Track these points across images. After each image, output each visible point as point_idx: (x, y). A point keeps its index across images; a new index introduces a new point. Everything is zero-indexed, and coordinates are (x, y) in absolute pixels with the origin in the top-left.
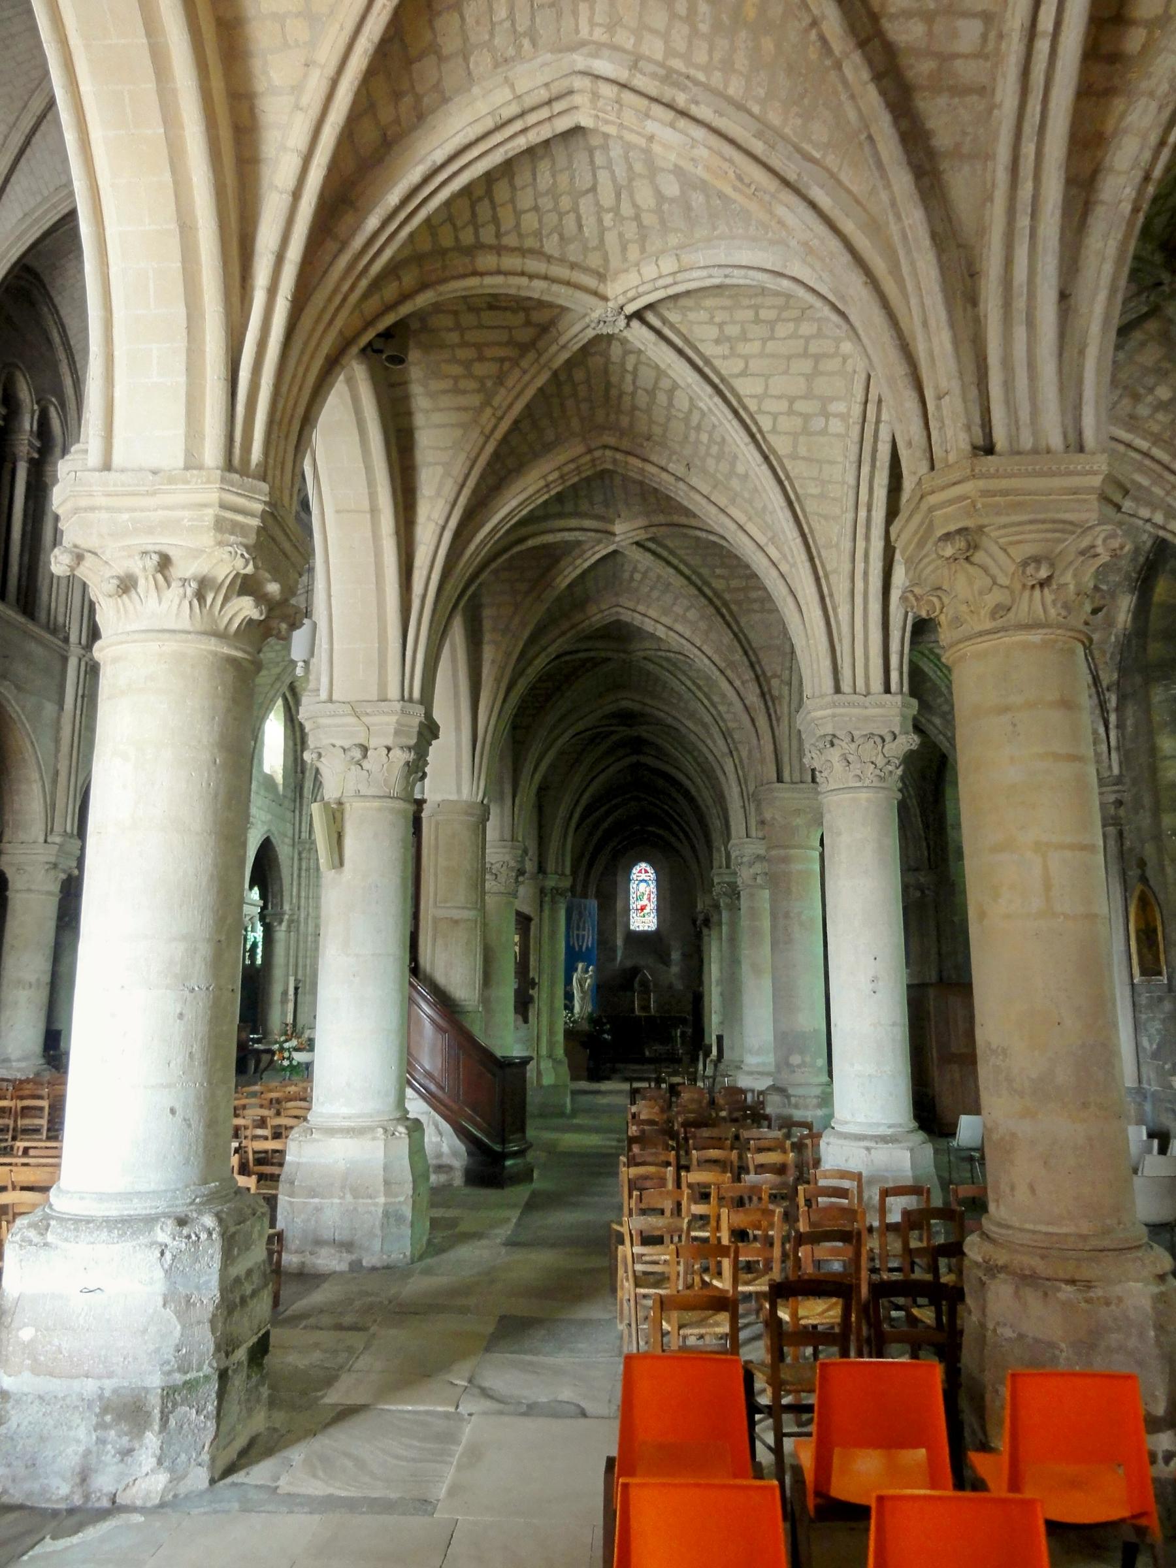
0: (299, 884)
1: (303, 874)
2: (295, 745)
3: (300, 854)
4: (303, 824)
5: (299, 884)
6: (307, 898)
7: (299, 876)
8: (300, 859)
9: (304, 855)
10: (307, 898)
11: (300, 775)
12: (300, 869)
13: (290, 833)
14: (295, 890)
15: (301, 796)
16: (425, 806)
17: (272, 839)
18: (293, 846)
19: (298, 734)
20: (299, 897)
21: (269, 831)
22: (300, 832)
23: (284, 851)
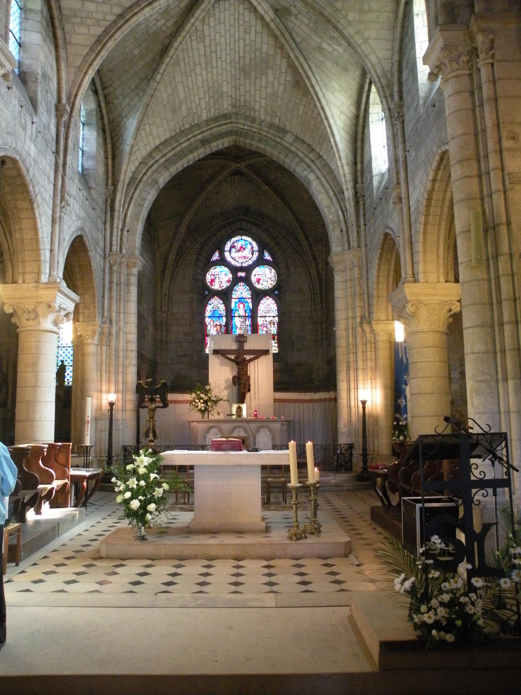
0: (110, 298)
1: (114, 287)
2: (106, 158)
3: (111, 267)
4: (114, 238)
5: (110, 298)
6: (118, 312)
7: (110, 290)
8: (111, 273)
9: (115, 268)
10: (118, 312)
11: (111, 188)
13: (101, 243)
14: (106, 303)
15: (112, 210)
17: (85, 238)
18: (104, 258)
19: (109, 146)
20: (110, 310)
21: (82, 229)
22: (111, 245)
23: (96, 259)
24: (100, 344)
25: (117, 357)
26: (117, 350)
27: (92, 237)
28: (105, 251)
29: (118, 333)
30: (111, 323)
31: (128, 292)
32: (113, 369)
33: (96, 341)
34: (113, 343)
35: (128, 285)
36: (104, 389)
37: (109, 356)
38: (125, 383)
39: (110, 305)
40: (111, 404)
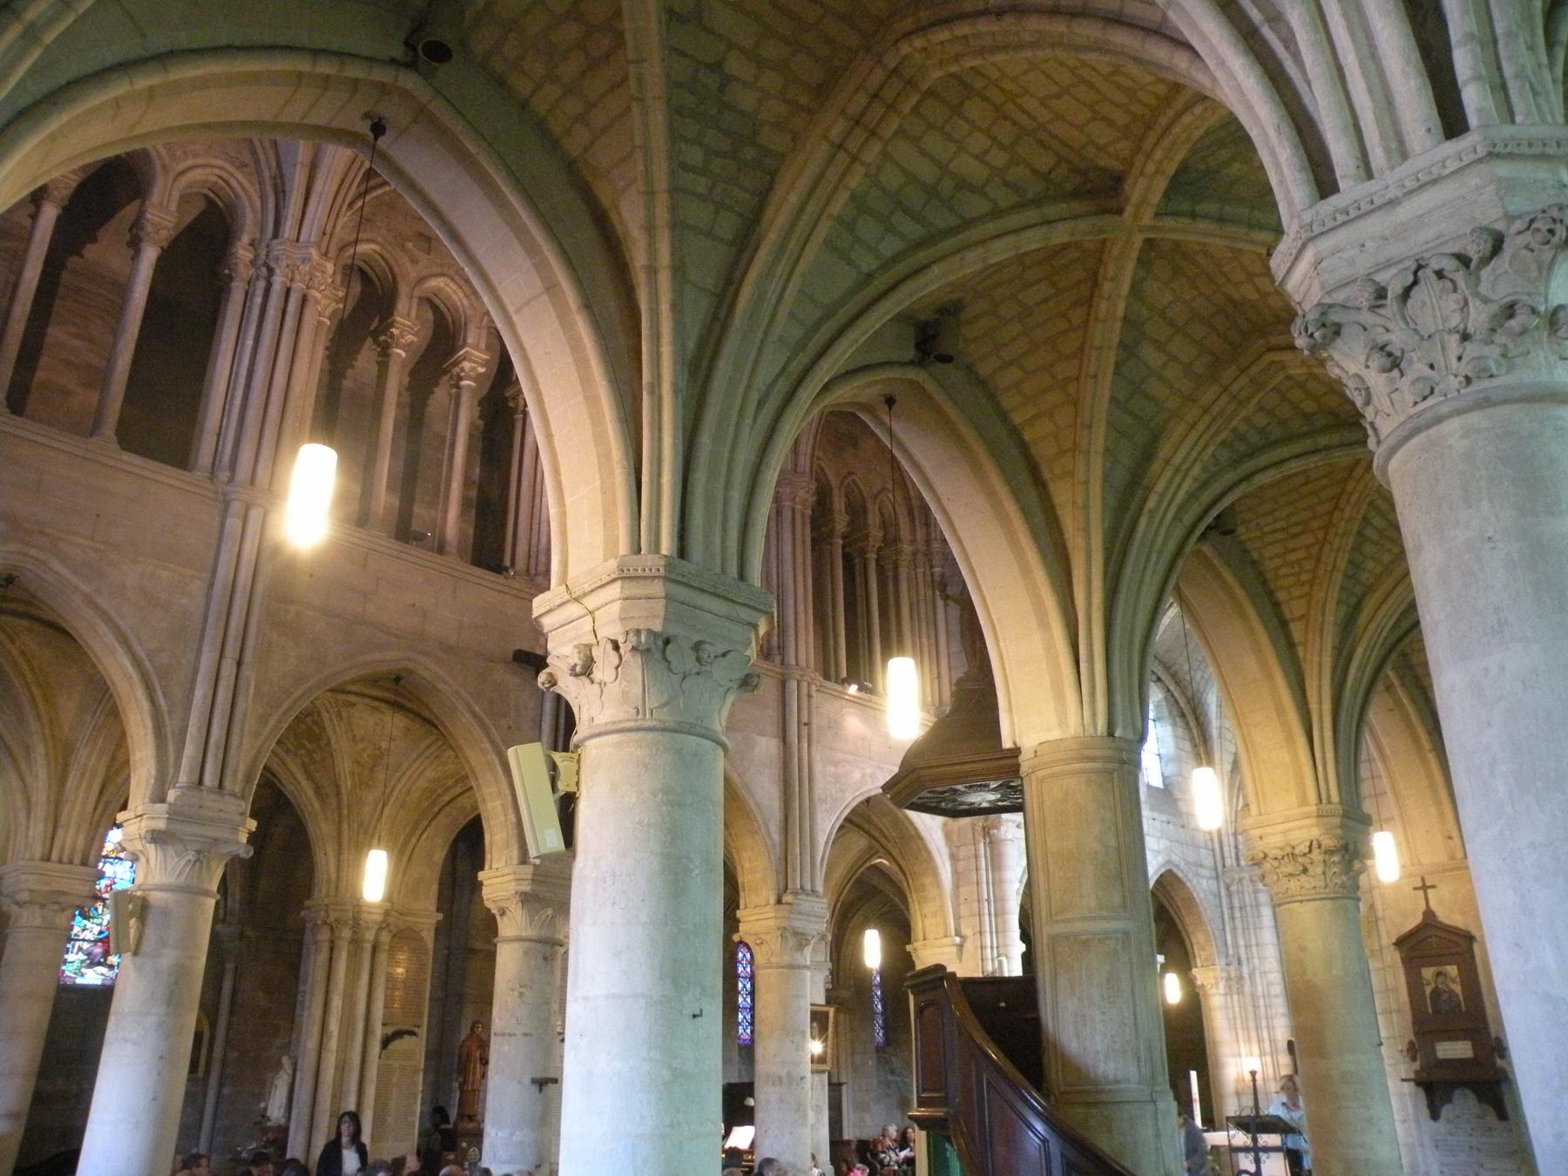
0: (1234, 929)
1: (1237, 914)
3: (1228, 888)
5: (1234, 929)
7: (1232, 918)
8: (1230, 895)
9: (1234, 888)
12: (1232, 908)
14: (1229, 937)
16: (1021, 758)
18: (1217, 878)
20: (1236, 945)
21: (1169, 862)
22: (1223, 858)
24: (1229, 992)
25: (1255, 1007)
26: (1254, 997)
27: (1187, 863)
28: (1216, 869)
29: (1252, 975)
30: (1240, 963)
31: (1259, 916)
32: (1252, 1025)
33: (1222, 990)
34: (1247, 989)
35: (1258, 906)
36: (1244, 1051)
37: (1243, 1007)
38: (1272, 1041)
39: (1235, 938)
40: (1253, 1074)
